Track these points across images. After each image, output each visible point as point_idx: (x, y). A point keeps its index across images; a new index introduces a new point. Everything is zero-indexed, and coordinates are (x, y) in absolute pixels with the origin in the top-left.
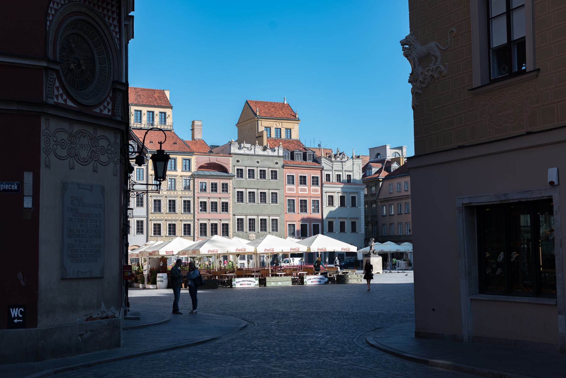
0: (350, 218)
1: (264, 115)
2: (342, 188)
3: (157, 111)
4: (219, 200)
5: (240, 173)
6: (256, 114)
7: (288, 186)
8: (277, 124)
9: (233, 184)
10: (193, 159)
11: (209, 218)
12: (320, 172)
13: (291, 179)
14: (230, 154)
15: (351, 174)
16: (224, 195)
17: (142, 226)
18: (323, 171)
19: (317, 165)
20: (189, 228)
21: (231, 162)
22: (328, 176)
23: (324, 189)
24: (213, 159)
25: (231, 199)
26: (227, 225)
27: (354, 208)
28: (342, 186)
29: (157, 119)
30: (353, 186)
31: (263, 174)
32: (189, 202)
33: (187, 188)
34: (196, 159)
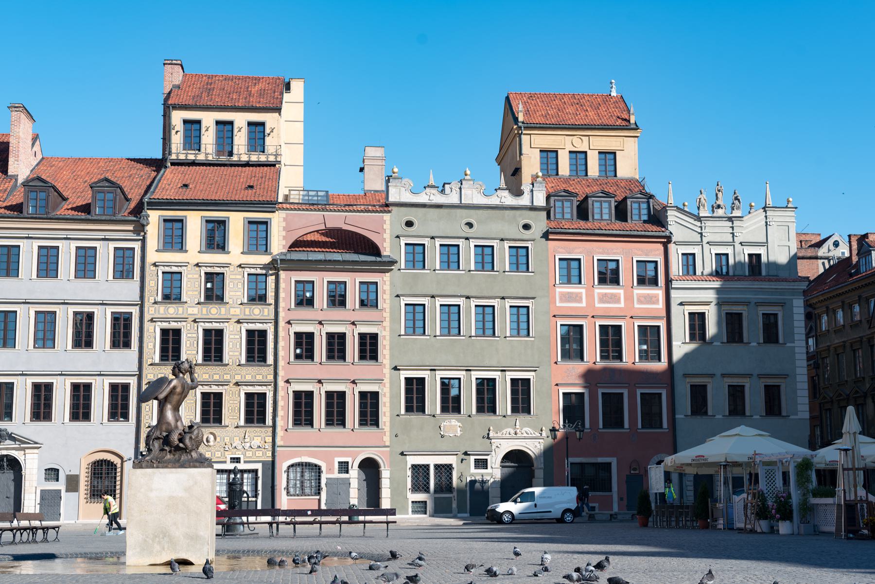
0: (760, 376)
1: (538, 119)
2: (718, 291)
3: (240, 120)
4: (319, 327)
5: (417, 255)
6: (516, 119)
7: (561, 290)
8: (576, 140)
9: (392, 284)
10: (277, 220)
11: (321, 377)
12: (660, 247)
13: (571, 270)
14: (387, 206)
15: (761, 251)
16: (368, 314)
17: (126, 398)
18: (672, 247)
19: (653, 229)
20: (263, 405)
21: (387, 226)
22: (689, 259)
23: (674, 294)
24: (337, 220)
25: (387, 324)
26: (375, 395)
27: (771, 347)
28: (717, 284)
29: (241, 140)
30: (766, 285)
31: (486, 257)
32: (263, 334)
33: (258, 298)
34: (285, 219)
